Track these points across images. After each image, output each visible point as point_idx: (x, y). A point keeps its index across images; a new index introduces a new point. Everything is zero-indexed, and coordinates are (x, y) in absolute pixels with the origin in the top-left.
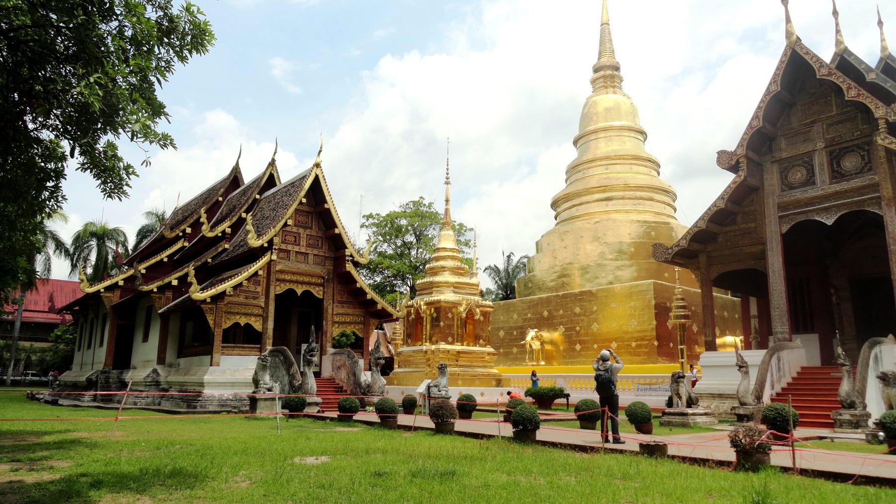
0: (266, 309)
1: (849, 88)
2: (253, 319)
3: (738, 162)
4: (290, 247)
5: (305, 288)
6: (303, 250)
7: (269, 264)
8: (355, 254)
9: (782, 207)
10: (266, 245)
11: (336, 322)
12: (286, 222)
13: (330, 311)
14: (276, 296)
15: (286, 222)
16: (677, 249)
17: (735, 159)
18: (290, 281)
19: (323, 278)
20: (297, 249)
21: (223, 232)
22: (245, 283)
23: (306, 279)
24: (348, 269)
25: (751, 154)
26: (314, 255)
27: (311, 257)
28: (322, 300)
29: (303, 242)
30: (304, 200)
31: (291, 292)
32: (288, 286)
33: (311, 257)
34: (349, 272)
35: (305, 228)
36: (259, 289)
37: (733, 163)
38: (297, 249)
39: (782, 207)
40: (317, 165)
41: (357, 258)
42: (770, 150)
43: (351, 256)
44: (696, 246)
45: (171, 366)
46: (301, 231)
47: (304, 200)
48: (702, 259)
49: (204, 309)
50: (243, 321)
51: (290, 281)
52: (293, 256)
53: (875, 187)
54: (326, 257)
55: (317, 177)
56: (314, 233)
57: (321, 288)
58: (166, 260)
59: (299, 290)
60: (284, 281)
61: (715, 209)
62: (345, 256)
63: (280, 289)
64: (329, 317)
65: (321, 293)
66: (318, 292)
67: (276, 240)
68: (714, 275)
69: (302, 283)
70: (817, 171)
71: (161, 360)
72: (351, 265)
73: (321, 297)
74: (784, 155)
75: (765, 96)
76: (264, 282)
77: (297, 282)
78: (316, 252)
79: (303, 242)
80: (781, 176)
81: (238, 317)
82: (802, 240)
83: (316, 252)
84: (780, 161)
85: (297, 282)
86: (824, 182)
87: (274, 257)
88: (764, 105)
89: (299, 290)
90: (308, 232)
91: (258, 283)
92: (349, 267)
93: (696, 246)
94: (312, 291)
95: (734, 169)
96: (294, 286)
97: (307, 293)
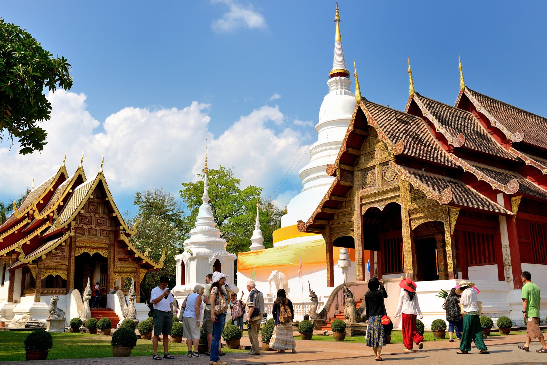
0: (69, 266)
1: (380, 133)
2: (61, 272)
3: (335, 172)
4: (85, 226)
5: (95, 251)
6: (94, 227)
7: (70, 237)
8: (126, 229)
9: (361, 198)
10: (67, 227)
11: (116, 272)
12: (80, 211)
13: (112, 264)
14: (77, 258)
15: (80, 211)
16: (308, 224)
17: (334, 169)
18: (86, 247)
21: (48, 216)
22: (53, 251)
24: (121, 239)
25: (343, 167)
26: (101, 230)
27: (99, 232)
28: (107, 259)
29: (94, 222)
30: (92, 197)
31: (86, 254)
32: (84, 250)
33: (99, 232)
34: (123, 241)
35: (95, 213)
36: (65, 254)
37: (333, 172)
38: (89, 227)
39: (361, 198)
41: (128, 231)
42: (357, 164)
43: (124, 230)
44: (320, 222)
45: (16, 302)
46: (92, 215)
47: (92, 197)
48: (327, 229)
49: (30, 268)
50: (55, 274)
51: (86, 247)
52: (87, 232)
53: (398, 189)
54: (109, 231)
55: (100, 181)
56: (101, 216)
57: (106, 251)
58: (16, 232)
60: (81, 247)
61: (325, 200)
62: (119, 230)
63: (79, 252)
64: (111, 270)
65: (106, 254)
66: (104, 253)
67: (73, 223)
68: (333, 240)
70: (377, 178)
71: (10, 299)
72: (124, 236)
73: (106, 257)
74: (363, 167)
75: (347, 132)
76: (68, 249)
77: (90, 247)
78: (102, 228)
79: (94, 222)
80: (362, 179)
81: (51, 271)
82: (371, 217)
83: (102, 228)
84: (362, 170)
85: (90, 247)
86: (379, 185)
87: (72, 234)
88: (346, 138)
89: (92, 252)
90: (97, 215)
91: (63, 250)
92: (123, 237)
93: (320, 222)
94: (100, 253)
95: (334, 175)
96: (87, 250)
97: (97, 254)
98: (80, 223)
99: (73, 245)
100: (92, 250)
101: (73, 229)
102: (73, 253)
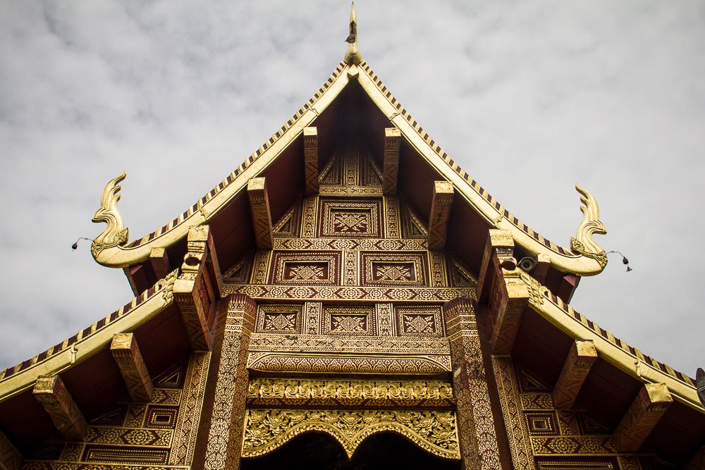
4: (300, 293)
5: (374, 424)
19: (447, 377)
20: (328, 294)
23: (379, 392)
26: (398, 305)
27: (385, 315)
32: (300, 424)
33: (385, 315)
40: (353, 60)
46: (342, 245)
57: (448, 419)
59: (351, 435)
69: (363, 407)
73: (456, 454)
89: (351, 435)
90: (368, 244)
94: (411, 433)
98: (273, 280)
99: (226, 390)
100: (349, 419)
101: (193, 261)
102: (219, 432)
